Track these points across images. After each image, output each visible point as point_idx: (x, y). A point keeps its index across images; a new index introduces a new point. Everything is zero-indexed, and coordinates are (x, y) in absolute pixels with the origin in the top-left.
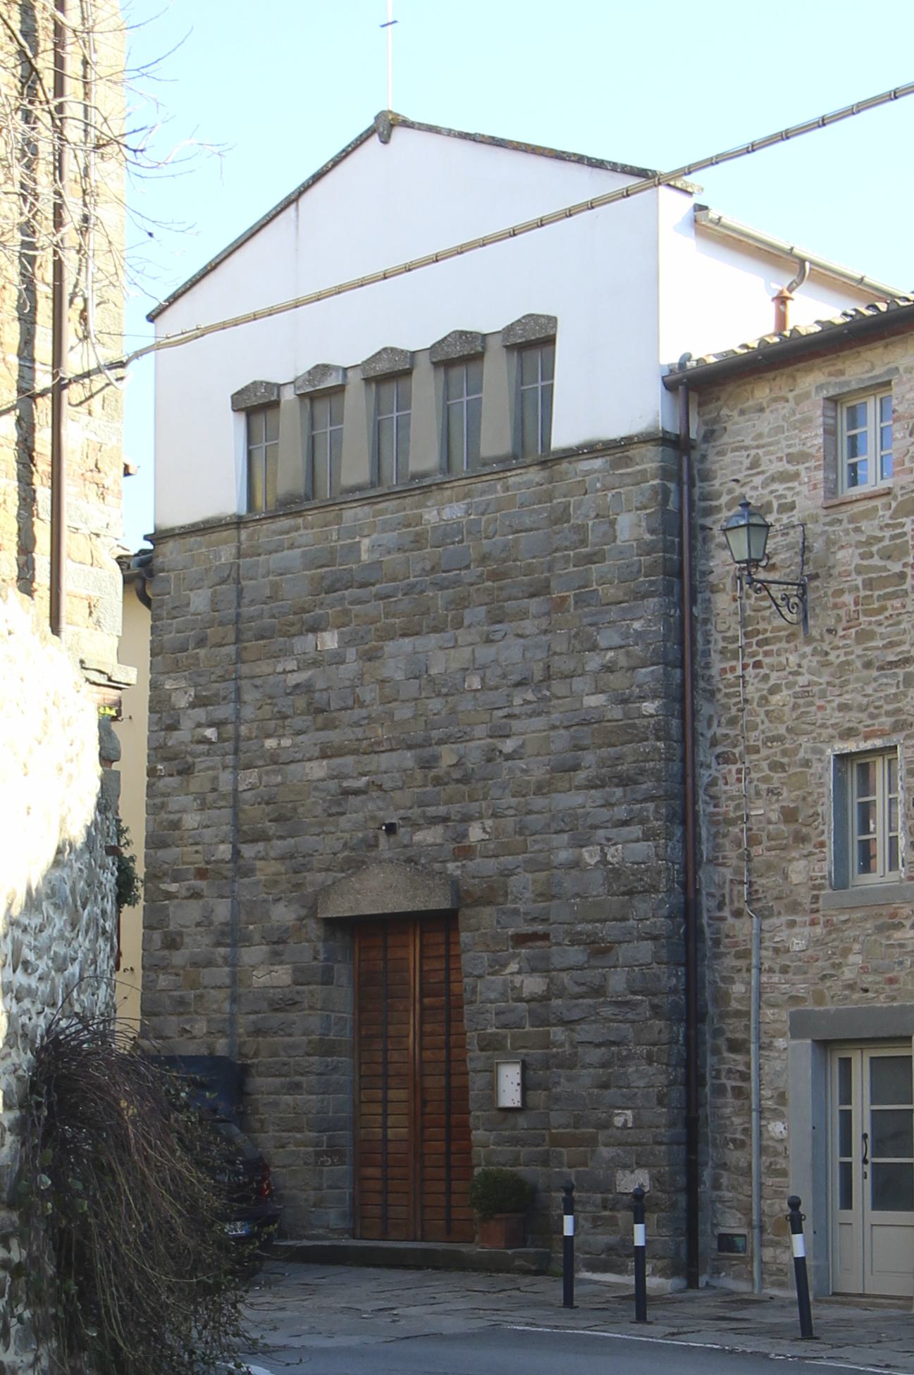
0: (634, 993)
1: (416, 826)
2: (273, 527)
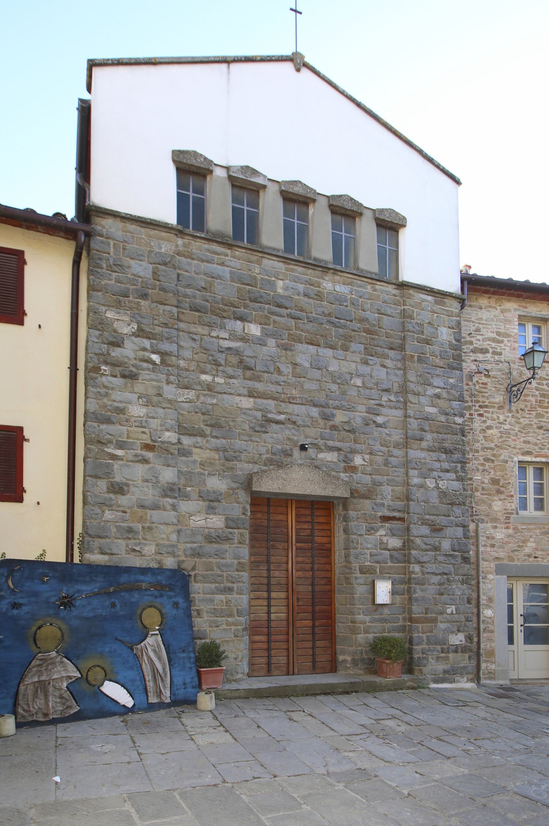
0: (454, 551)
1: (319, 449)
2: (206, 246)
